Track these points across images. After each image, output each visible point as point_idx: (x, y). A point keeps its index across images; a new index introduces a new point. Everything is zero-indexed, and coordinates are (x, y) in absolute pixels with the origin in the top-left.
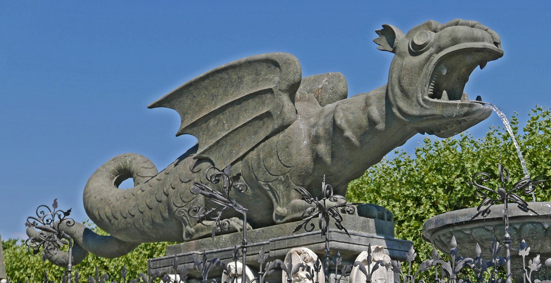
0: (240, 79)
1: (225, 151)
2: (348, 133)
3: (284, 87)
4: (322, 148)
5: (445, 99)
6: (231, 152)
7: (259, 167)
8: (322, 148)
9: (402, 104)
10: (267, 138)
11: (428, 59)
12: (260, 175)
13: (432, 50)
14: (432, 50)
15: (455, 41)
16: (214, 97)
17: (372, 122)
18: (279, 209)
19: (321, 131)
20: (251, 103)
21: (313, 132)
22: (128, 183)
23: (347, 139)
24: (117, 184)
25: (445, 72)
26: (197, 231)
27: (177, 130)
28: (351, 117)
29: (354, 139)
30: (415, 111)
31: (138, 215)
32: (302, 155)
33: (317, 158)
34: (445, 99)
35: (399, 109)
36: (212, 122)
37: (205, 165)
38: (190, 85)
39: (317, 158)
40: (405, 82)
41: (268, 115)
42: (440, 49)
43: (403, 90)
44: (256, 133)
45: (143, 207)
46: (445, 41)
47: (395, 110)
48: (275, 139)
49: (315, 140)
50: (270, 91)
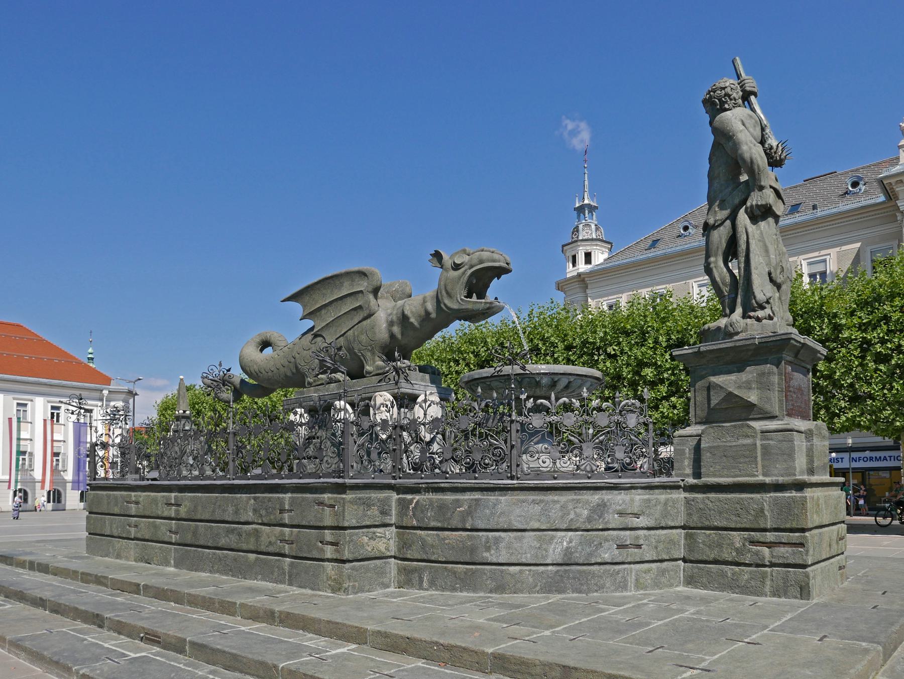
0: (342, 284)
2: (412, 320)
3: (370, 289)
5: (474, 298)
6: (336, 331)
7: (354, 340)
8: (396, 330)
9: (447, 301)
10: (359, 322)
11: (464, 273)
13: (466, 267)
14: (466, 267)
15: (481, 262)
16: (324, 295)
17: (428, 313)
18: (368, 368)
20: (349, 300)
22: (268, 351)
23: (412, 323)
24: (261, 350)
25: (474, 281)
26: (315, 381)
27: (300, 316)
28: (414, 310)
29: (416, 324)
33: (392, 336)
34: (474, 298)
35: (445, 305)
36: (323, 312)
37: (319, 339)
39: (392, 336)
40: (449, 288)
41: (360, 307)
43: (447, 293)
44: (352, 319)
45: (279, 366)
46: (475, 261)
47: (442, 306)
48: (364, 323)
49: (391, 324)
50: (361, 292)
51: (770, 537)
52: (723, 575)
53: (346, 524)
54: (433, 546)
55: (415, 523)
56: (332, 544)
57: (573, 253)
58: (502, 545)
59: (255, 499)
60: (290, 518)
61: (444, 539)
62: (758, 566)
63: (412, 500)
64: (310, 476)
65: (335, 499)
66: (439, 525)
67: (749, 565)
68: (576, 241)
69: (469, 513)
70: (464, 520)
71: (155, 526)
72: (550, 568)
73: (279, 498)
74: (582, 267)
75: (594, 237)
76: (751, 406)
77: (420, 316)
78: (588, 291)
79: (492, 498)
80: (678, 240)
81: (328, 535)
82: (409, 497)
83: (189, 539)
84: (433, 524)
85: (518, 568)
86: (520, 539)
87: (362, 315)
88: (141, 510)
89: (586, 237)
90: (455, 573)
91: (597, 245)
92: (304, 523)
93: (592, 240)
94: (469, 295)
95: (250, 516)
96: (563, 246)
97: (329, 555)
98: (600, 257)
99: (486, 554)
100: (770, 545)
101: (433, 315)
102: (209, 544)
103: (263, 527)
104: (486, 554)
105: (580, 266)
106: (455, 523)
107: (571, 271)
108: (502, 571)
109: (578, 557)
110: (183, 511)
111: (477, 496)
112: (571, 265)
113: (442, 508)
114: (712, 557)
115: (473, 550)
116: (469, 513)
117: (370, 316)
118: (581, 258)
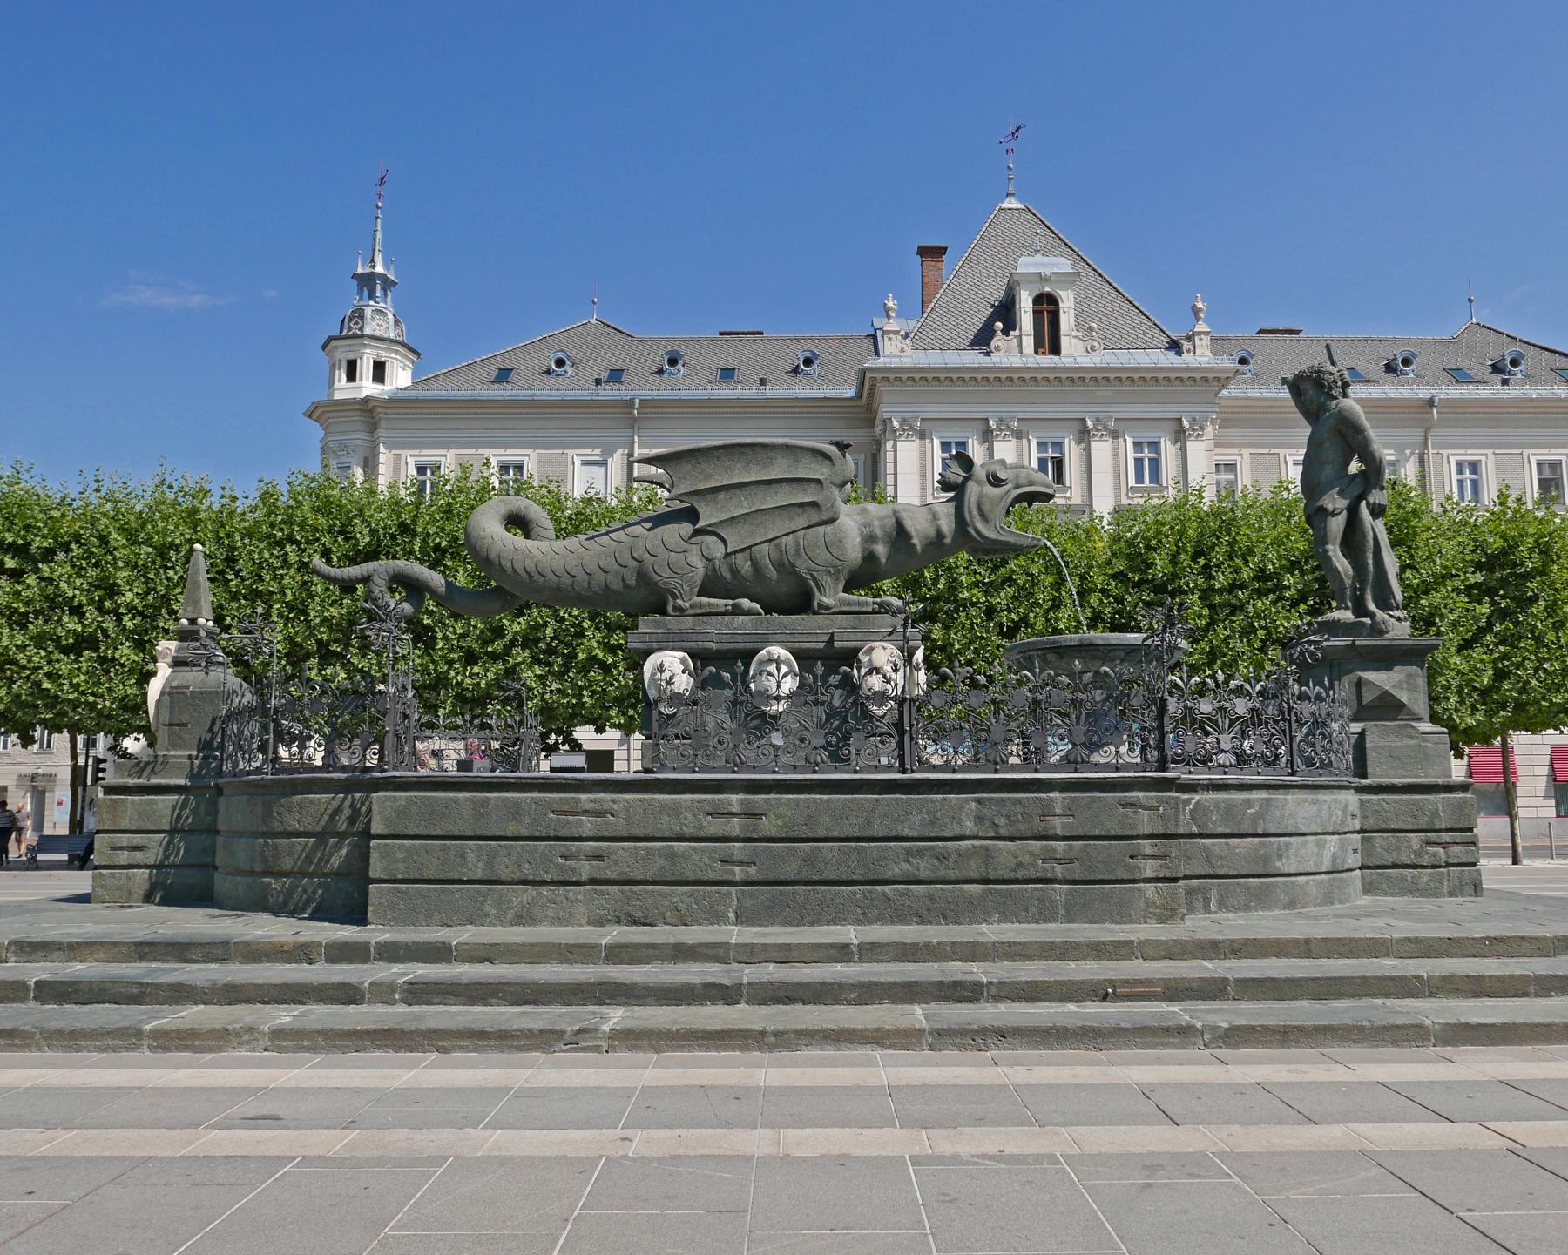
1: (744, 529)
2: (915, 541)
4: (881, 550)
7: (797, 551)
8: (881, 550)
9: (980, 525)
12: (798, 563)
13: (1010, 486)
14: (1010, 486)
15: (1031, 484)
17: (940, 535)
19: (878, 532)
21: (866, 531)
26: (692, 606)
30: (992, 535)
31: (581, 575)
32: (854, 553)
33: (870, 557)
35: (977, 531)
36: (722, 496)
38: (699, 450)
39: (870, 557)
40: (986, 508)
41: (814, 504)
42: (1017, 487)
45: (592, 567)
46: (1022, 481)
48: (821, 529)
49: (870, 539)
50: (818, 482)
51: (1446, 837)
52: (1404, 879)
53: (1181, 831)
54: (1221, 858)
55: (1195, 829)
56: (1154, 858)
57: (351, 357)
58: (1291, 852)
59: (979, 801)
60: (1064, 826)
62: (1434, 867)
63: (1187, 802)
64: (935, 768)
65: (1160, 800)
66: (1228, 831)
67: (1426, 867)
68: (362, 336)
69: (1260, 816)
71: (671, 856)
72: (1323, 876)
73: (1040, 799)
74: (367, 387)
75: (392, 336)
77: (927, 537)
78: (381, 433)
79: (1279, 796)
80: (551, 380)
81: (1147, 847)
82: (1185, 796)
83: (791, 870)
84: (1220, 830)
86: (1304, 844)
87: (815, 518)
88: (618, 825)
89: (377, 333)
91: (397, 352)
92: (1097, 832)
93: (391, 341)
95: (969, 826)
96: (330, 339)
97: (1148, 874)
98: (400, 377)
99: (1278, 864)
100: (1445, 845)
101: (948, 540)
102: (855, 877)
103: (1001, 843)
104: (1278, 864)
105: (365, 383)
106: (1246, 828)
107: (343, 389)
110: (767, 825)
111: (1263, 794)
112: (344, 377)
113: (1229, 811)
114: (1390, 861)
115: (1265, 859)
116: (1260, 816)
117: (832, 520)
118: (366, 369)
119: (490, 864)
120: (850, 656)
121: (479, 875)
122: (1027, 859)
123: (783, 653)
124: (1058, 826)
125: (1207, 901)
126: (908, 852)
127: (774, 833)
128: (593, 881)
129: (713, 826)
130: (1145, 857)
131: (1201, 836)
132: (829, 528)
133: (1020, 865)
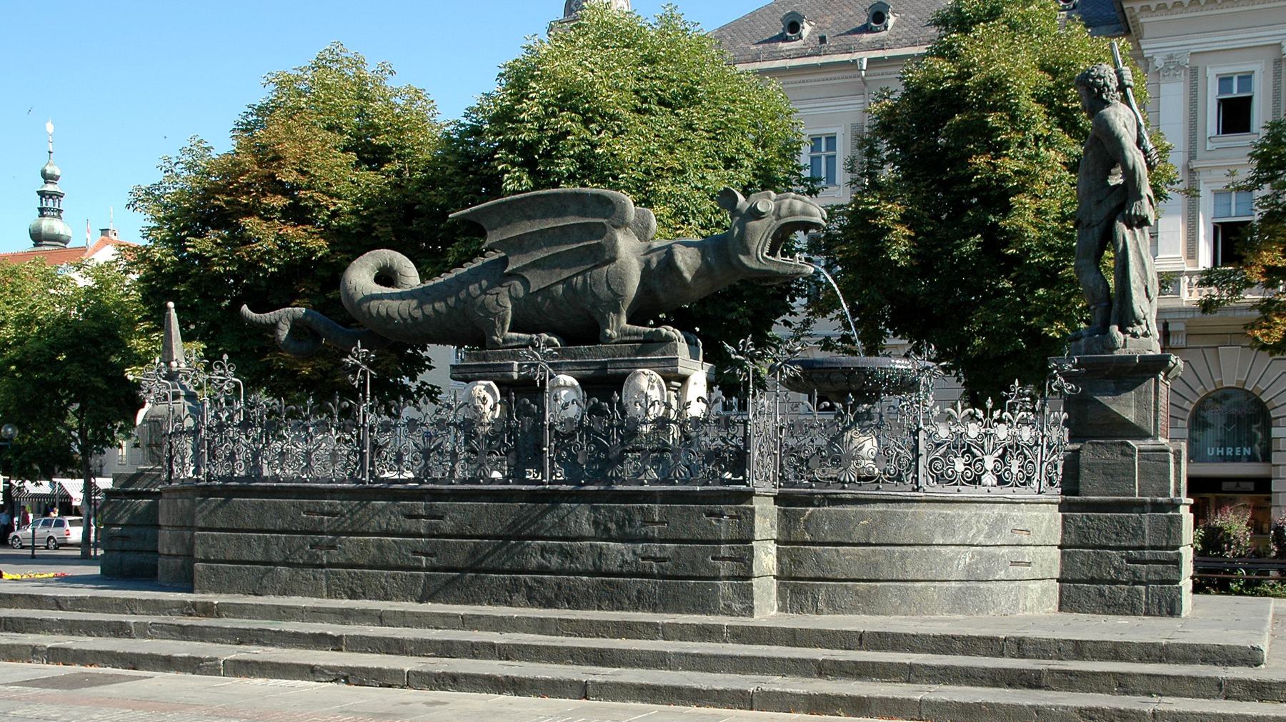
51: (1147, 554)
55: (808, 537)
61: (844, 555)
63: (802, 514)
70: (868, 536)
71: (380, 547)
72: (953, 584)
76: (1125, 423)
81: (724, 549)
84: (829, 539)
85: (923, 584)
90: (857, 593)
92: (685, 537)
94: (772, 252)
108: (907, 589)
109: (981, 573)
110: (447, 525)
115: (876, 565)
119: (266, 550)
120: (617, 382)
121: (260, 557)
122: (629, 557)
123: (570, 380)
124: (655, 530)
125: (815, 600)
126: (543, 549)
127: (448, 530)
128: (330, 565)
129: (409, 524)
130: (723, 559)
131: (813, 543)
132: (612, 266)
133: (625, 562)
